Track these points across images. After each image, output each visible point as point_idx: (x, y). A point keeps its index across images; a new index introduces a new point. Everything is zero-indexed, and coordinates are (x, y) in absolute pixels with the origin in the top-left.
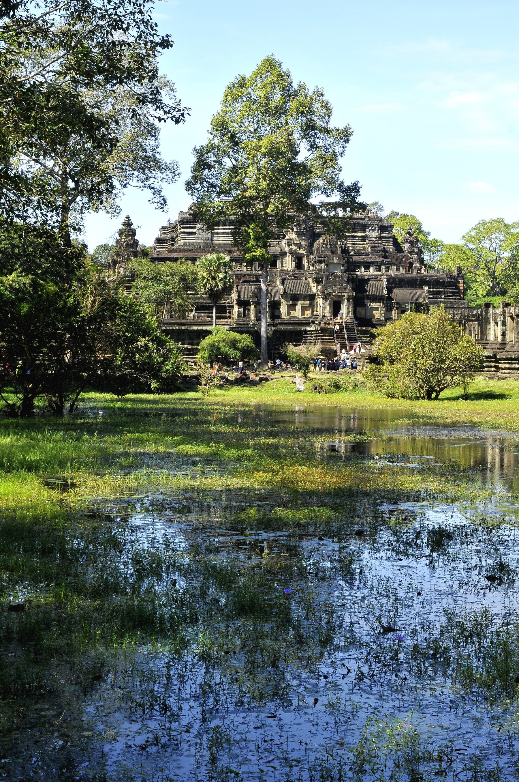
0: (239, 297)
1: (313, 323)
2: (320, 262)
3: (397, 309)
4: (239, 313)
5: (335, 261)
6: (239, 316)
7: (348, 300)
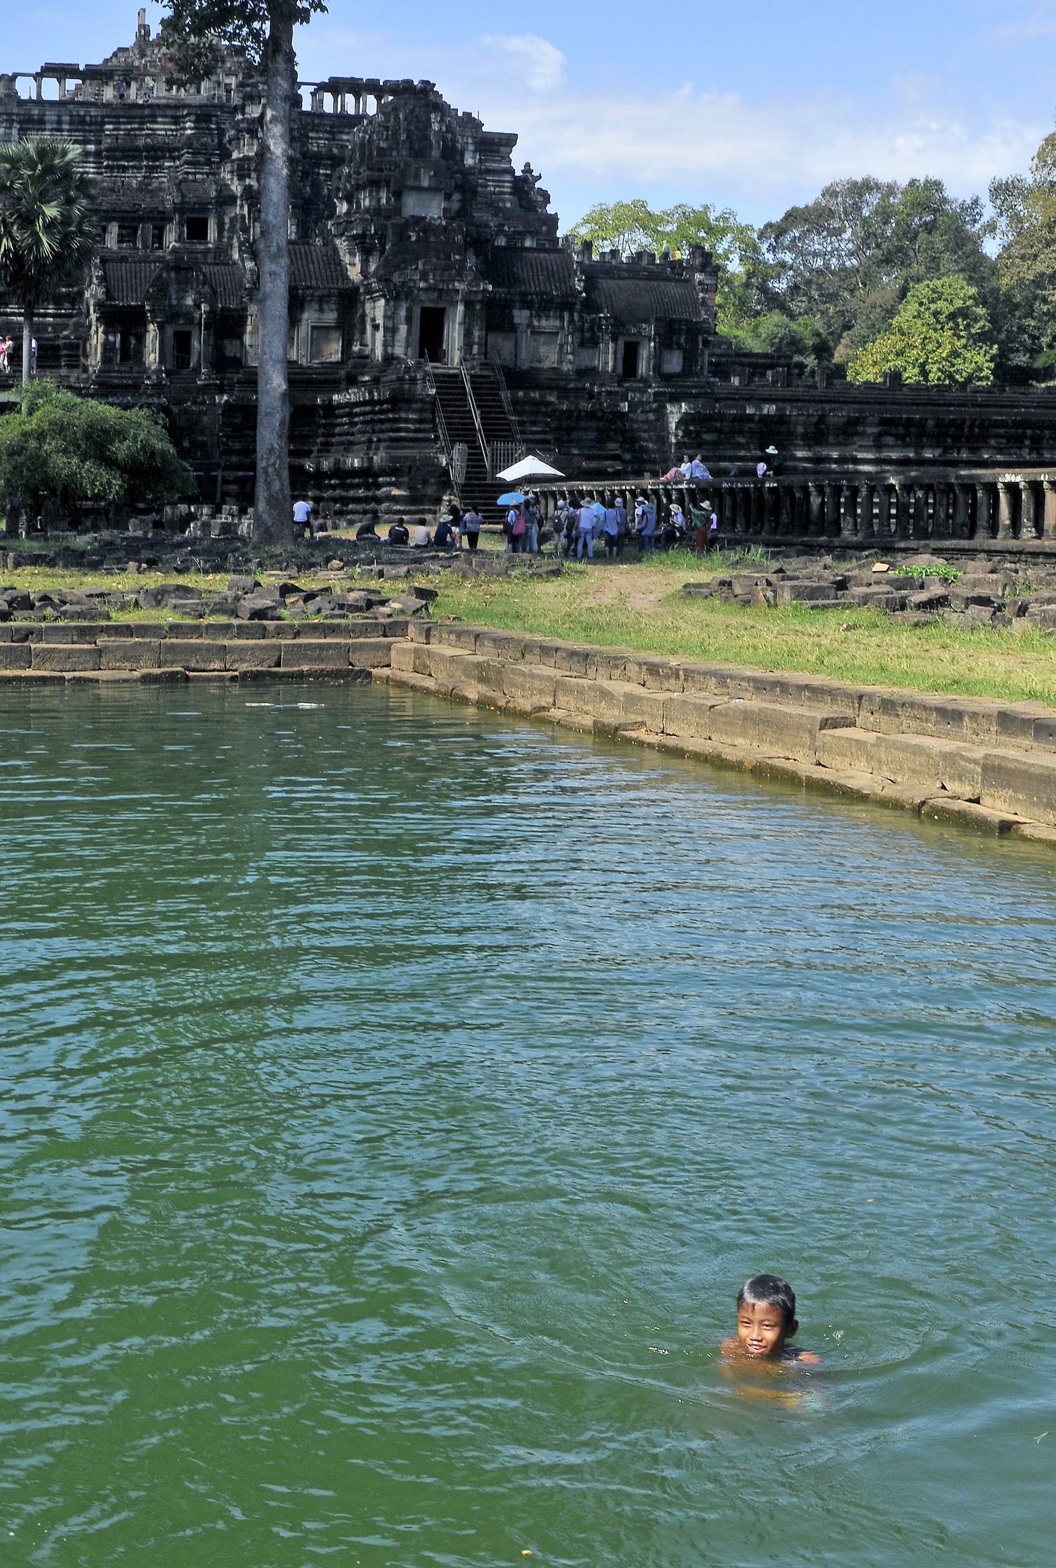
0: (108, 293)
1: (352, 381)
2: (374, 184)
3: (615, 340)
4: (107, 347)
5: (425, 183)
6: (106, 359)
7: (468, 304)
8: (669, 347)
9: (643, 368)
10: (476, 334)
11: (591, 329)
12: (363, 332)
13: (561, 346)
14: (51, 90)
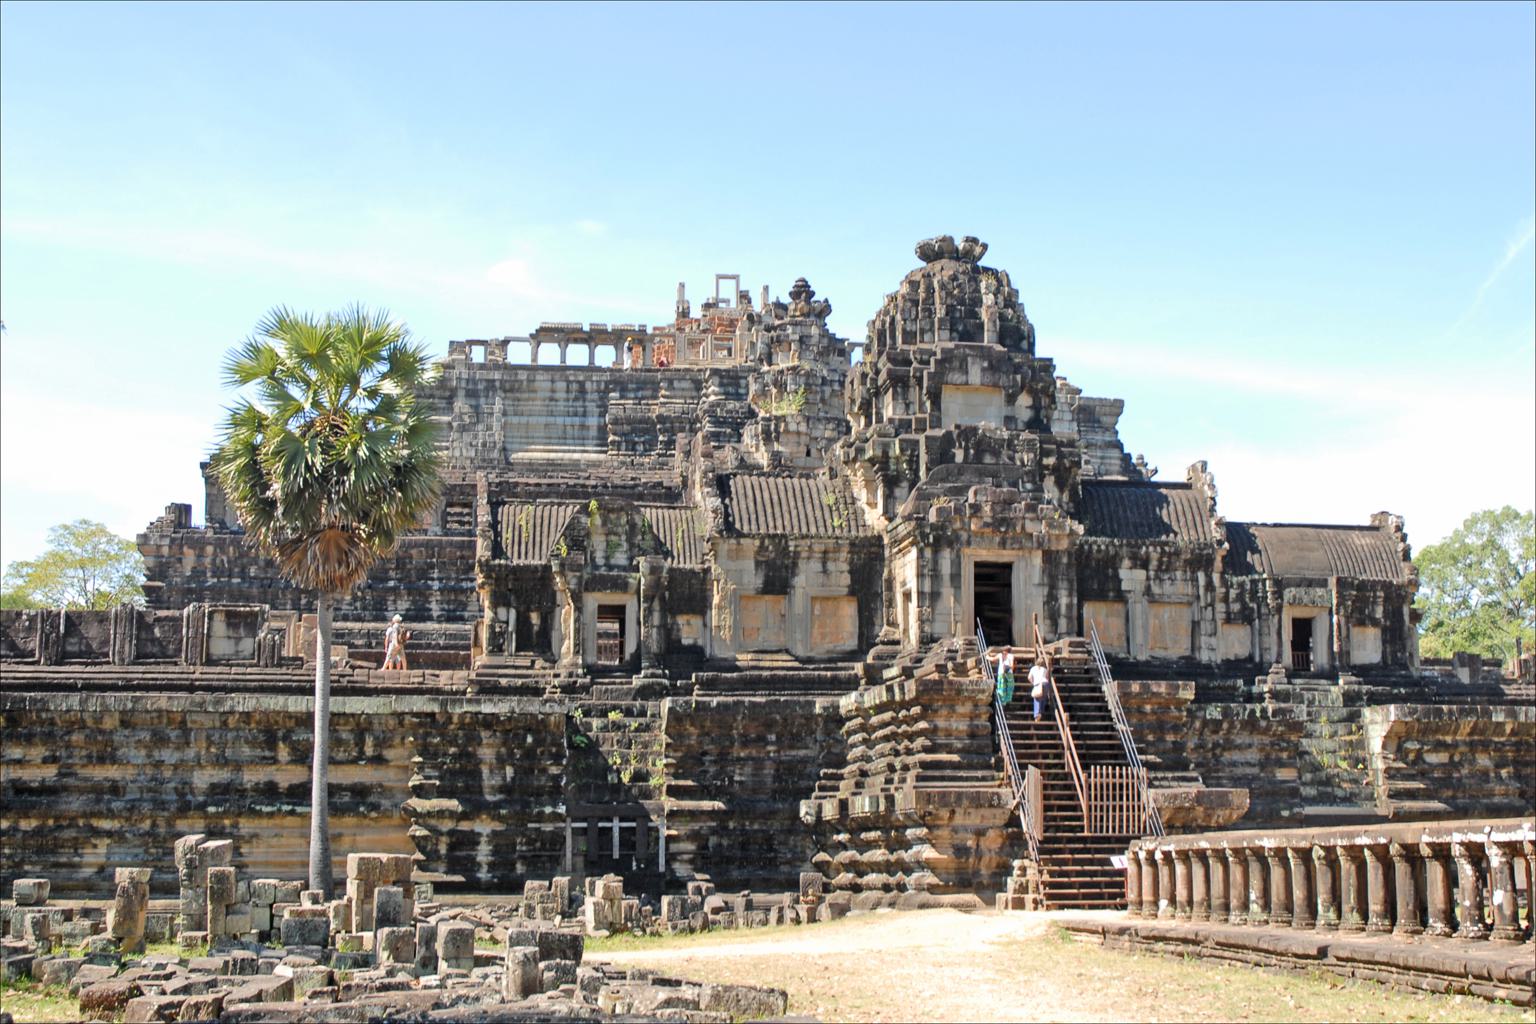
7: (1049, 557)
8: (1361, 623)
9: (1319, 657)
10: (1064, 601)
11: (1240, 598)
12: (891, 603)
13: (1195, 625)
14: (549, 354)
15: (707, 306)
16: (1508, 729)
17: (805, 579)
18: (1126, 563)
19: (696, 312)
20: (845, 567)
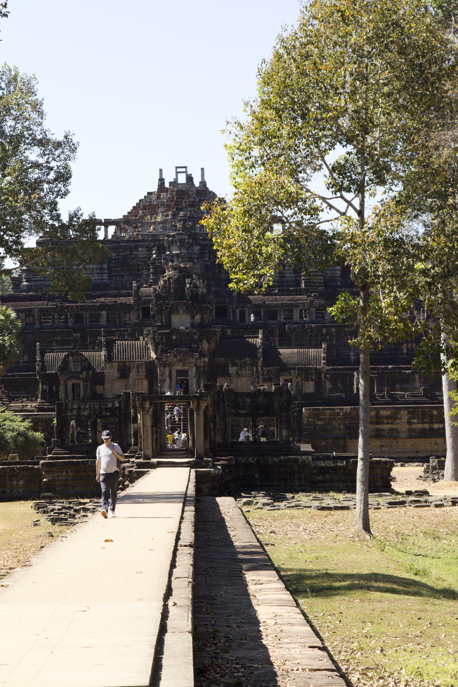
7: (198, 368)
8: (307, 380)
11: (268, 374)
15: (171, 183)
16: (341, 414)
17: (133, 374)
18: (230, 365)
19: (167, 185)
20: (144, 370)
